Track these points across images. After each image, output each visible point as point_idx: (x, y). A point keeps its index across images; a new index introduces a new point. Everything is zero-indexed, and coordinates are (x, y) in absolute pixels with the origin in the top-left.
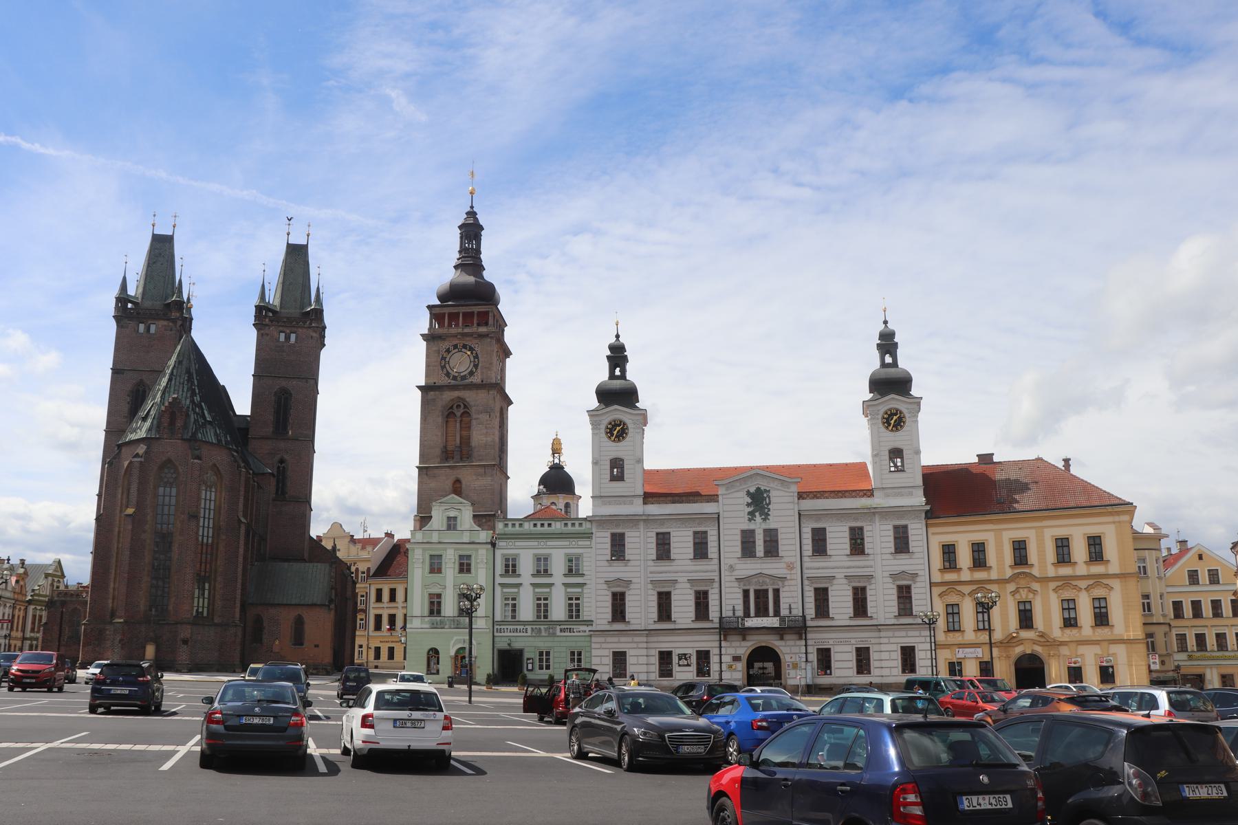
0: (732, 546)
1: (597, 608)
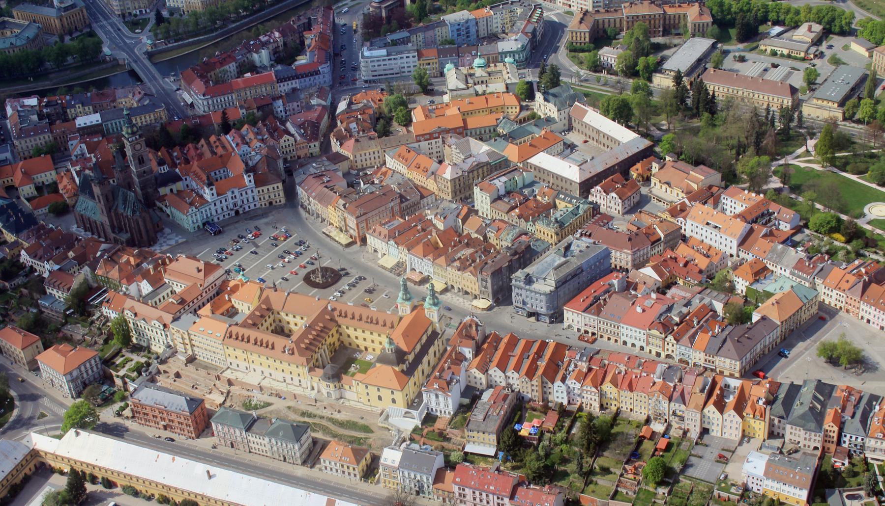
0: (230, 199)
1: (214, 213)
